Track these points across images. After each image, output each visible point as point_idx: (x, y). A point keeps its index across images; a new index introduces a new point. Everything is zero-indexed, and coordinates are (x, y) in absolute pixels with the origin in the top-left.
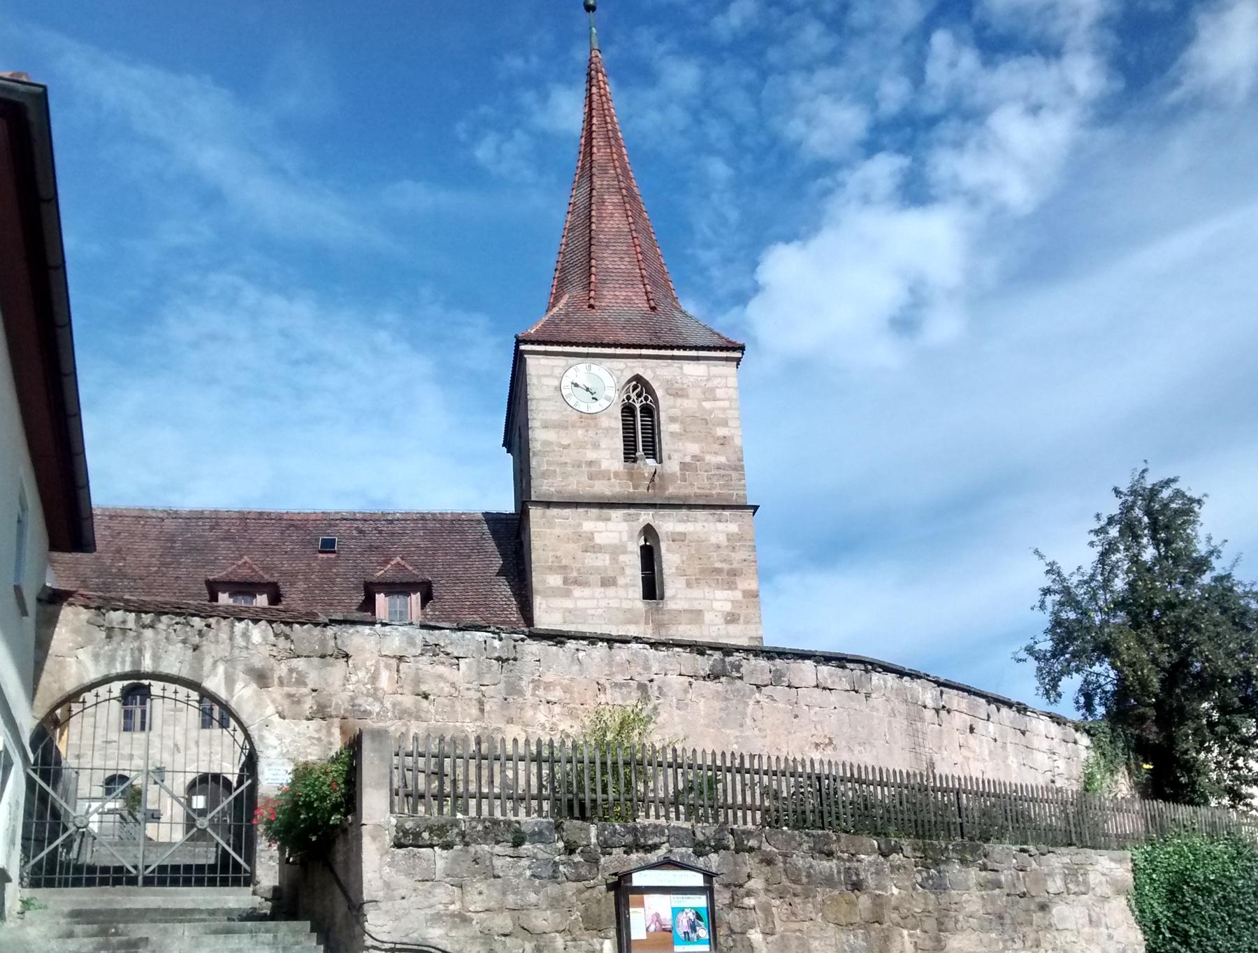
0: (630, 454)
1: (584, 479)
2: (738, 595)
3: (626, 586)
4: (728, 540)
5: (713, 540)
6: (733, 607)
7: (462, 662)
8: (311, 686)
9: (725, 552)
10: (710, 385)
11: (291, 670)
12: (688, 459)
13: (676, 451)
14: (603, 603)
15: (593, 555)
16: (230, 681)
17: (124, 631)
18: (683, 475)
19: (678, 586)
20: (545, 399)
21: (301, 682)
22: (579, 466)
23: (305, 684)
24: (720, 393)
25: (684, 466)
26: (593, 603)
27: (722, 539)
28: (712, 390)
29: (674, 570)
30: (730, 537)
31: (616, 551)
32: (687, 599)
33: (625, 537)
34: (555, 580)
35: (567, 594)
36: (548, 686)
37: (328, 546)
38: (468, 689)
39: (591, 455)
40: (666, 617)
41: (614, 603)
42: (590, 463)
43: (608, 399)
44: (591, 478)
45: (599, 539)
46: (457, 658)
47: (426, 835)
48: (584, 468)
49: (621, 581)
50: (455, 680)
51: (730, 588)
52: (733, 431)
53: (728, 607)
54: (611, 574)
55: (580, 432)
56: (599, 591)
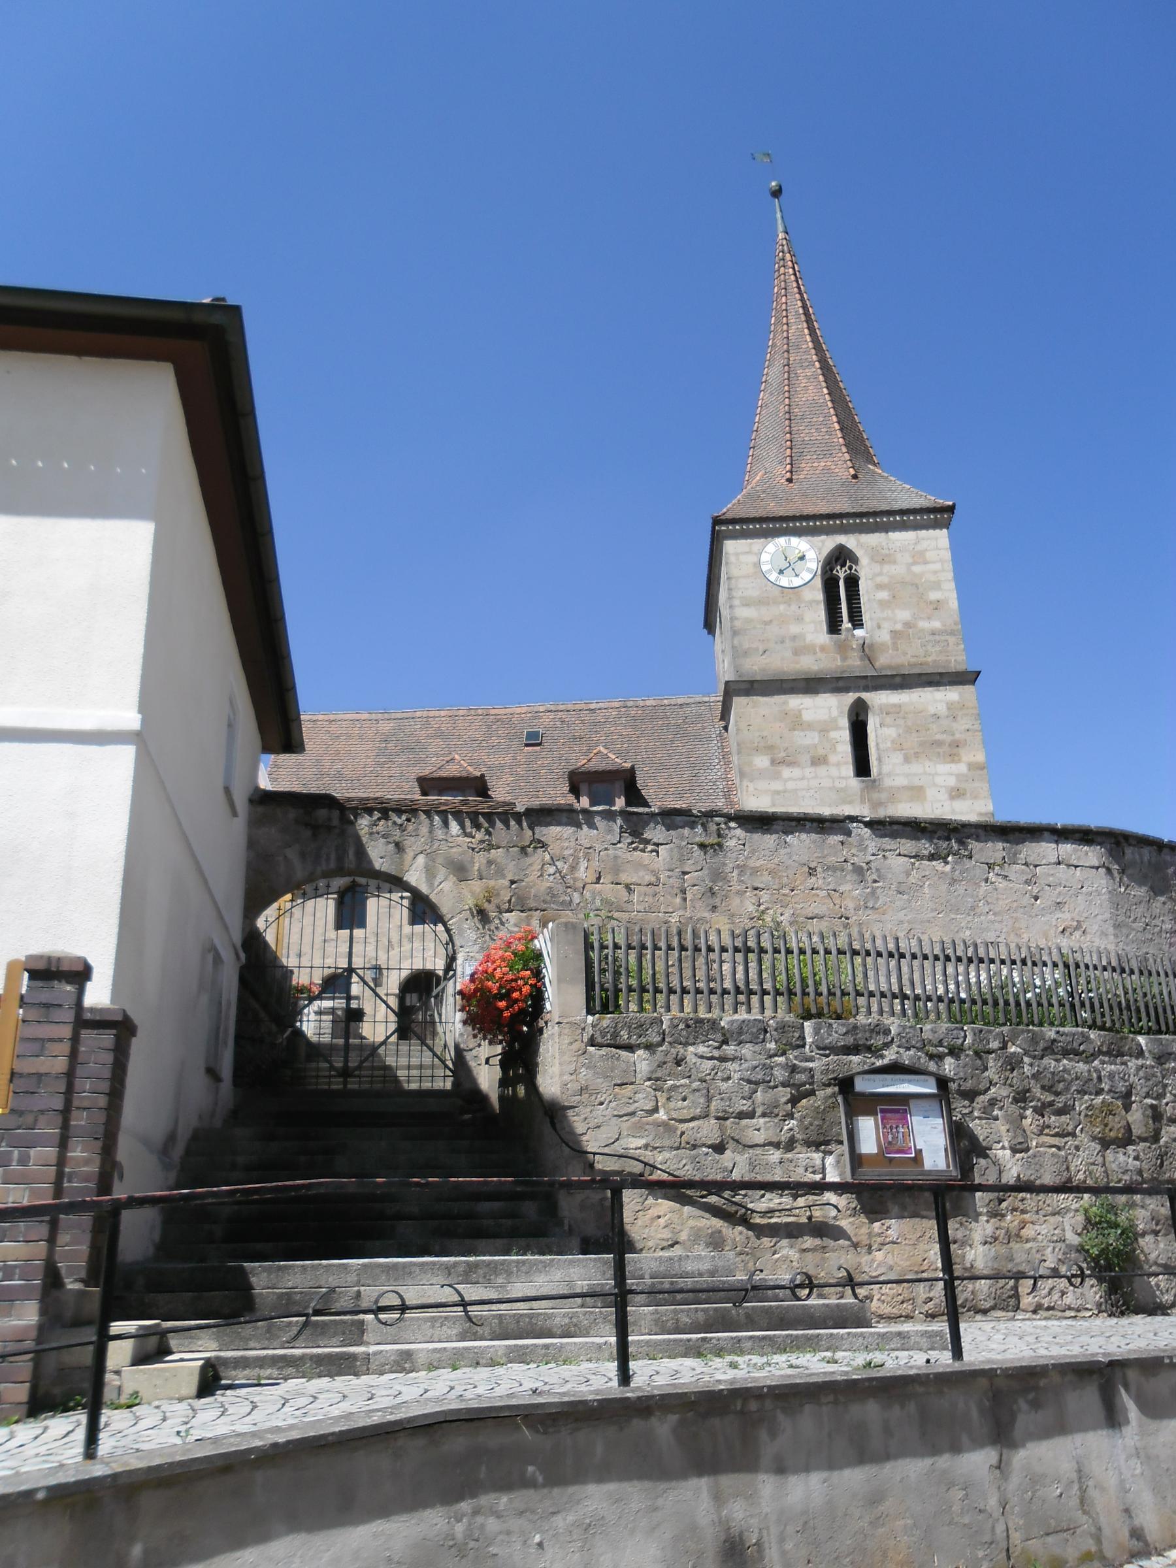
0: (834, 626)
1: (788, 654)
2: (962, 768)
3: (838, 765)
4: (949, 709)
5: (932, 710)
7: (661, 848)
8: (510, 877)
10: (919, 548)
11: (490, 863)
12: (899, 627)
13: (884, 619)
14: (814, 783)
15: (802, 734)
16: (430, 873)
17: (329, 828)
18: (894, 644)
21: (500, 873)
22: (782, 642)
23: (503, 877)
24: (930, 555)
25: (895, 634)
26: (804, 784)
27: (942, 709)
28: (922, 553)
29: (889, 744)
30: (950, 706)
31: (824, 729)
32: (907, 775)
33: (835, 713)
34: (762, 762)
35: (777, 776)
36: (755, 871)
37: (534, 740)
38: (669, 877)
39: (794, 629)
41: (827, 783)
42: (794, 638)
43: (809, 570)
44: (796, 652)
46: (658, 845)
47: (624, 1034)
49: (833, 759)
50: (655, 866)
51: (953, 761)
53: (952, 782)
54: (821, 752)
55: (782, 607)
56: (809, 771)
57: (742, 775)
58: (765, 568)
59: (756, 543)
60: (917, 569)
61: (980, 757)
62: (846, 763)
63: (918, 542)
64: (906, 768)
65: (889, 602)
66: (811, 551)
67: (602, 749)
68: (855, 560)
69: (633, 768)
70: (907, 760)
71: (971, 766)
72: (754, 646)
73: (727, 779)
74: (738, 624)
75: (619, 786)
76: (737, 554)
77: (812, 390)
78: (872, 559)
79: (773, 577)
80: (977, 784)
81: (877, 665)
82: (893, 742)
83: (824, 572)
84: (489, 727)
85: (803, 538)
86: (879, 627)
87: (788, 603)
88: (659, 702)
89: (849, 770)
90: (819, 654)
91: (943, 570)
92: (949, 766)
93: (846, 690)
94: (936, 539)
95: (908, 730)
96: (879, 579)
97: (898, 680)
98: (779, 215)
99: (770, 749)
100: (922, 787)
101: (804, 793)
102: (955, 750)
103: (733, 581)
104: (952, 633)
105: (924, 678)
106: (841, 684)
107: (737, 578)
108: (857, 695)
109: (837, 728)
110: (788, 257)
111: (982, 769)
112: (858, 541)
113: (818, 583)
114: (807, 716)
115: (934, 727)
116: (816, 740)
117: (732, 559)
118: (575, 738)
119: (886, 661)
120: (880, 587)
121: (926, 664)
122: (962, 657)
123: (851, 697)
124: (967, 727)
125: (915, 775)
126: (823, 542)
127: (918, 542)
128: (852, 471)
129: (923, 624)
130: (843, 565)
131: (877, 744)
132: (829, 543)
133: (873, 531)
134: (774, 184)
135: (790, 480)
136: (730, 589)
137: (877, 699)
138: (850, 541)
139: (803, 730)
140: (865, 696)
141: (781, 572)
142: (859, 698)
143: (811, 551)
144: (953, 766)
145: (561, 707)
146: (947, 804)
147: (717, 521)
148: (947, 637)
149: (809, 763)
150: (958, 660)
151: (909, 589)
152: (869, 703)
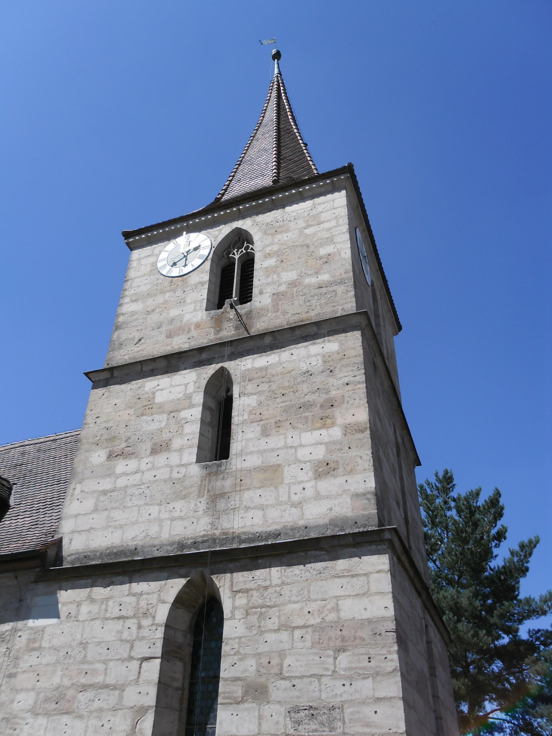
2: (336, 433)
3: (180, 450)
4: (325, 362)
5: (304, 367)
6: (330, 451)
9: (318, 379)
12: (283, 288)
14: (149, 476)
15: (149, 418)
19: (251, 435)
25: (277, 296)
27: (316, 363)
30: (326, 359)
34: (98, 457)
35: (110, 474)
39: (174, 313)
40: (228, 483)
41: (163, 474)
42: (172, 321)
44: (169, 336)
45: (160, 398)
49: (177, 443)
51: (324, 426)
52: (338, 246)
53: (320, 453)
54: (166, 436)
58: (159, 265)
60: (308, 231)
63: (314, 206)
64: (263, 444)
65: (276, 267)
70: (265, 433)
71: (348, 429)
80: (354, 453)
82: (250, 413)
85: (203, 232)
92: (316, 433)
93: (209, 362)
94: (333, 200)
100: (279, 465)
102: (329, 412)
104: (342, 282)
105: (298, 332)
115: (305, 388)
120: (268, 256)
123: (211, 370)
124: (346, 380)
125: (273, 450)
126: (220, 231)
127: (314, 206)
133: (270, 210)
138: (245, 224)
142: (222, 368)
144: (324, 432)
149: (149, 452)
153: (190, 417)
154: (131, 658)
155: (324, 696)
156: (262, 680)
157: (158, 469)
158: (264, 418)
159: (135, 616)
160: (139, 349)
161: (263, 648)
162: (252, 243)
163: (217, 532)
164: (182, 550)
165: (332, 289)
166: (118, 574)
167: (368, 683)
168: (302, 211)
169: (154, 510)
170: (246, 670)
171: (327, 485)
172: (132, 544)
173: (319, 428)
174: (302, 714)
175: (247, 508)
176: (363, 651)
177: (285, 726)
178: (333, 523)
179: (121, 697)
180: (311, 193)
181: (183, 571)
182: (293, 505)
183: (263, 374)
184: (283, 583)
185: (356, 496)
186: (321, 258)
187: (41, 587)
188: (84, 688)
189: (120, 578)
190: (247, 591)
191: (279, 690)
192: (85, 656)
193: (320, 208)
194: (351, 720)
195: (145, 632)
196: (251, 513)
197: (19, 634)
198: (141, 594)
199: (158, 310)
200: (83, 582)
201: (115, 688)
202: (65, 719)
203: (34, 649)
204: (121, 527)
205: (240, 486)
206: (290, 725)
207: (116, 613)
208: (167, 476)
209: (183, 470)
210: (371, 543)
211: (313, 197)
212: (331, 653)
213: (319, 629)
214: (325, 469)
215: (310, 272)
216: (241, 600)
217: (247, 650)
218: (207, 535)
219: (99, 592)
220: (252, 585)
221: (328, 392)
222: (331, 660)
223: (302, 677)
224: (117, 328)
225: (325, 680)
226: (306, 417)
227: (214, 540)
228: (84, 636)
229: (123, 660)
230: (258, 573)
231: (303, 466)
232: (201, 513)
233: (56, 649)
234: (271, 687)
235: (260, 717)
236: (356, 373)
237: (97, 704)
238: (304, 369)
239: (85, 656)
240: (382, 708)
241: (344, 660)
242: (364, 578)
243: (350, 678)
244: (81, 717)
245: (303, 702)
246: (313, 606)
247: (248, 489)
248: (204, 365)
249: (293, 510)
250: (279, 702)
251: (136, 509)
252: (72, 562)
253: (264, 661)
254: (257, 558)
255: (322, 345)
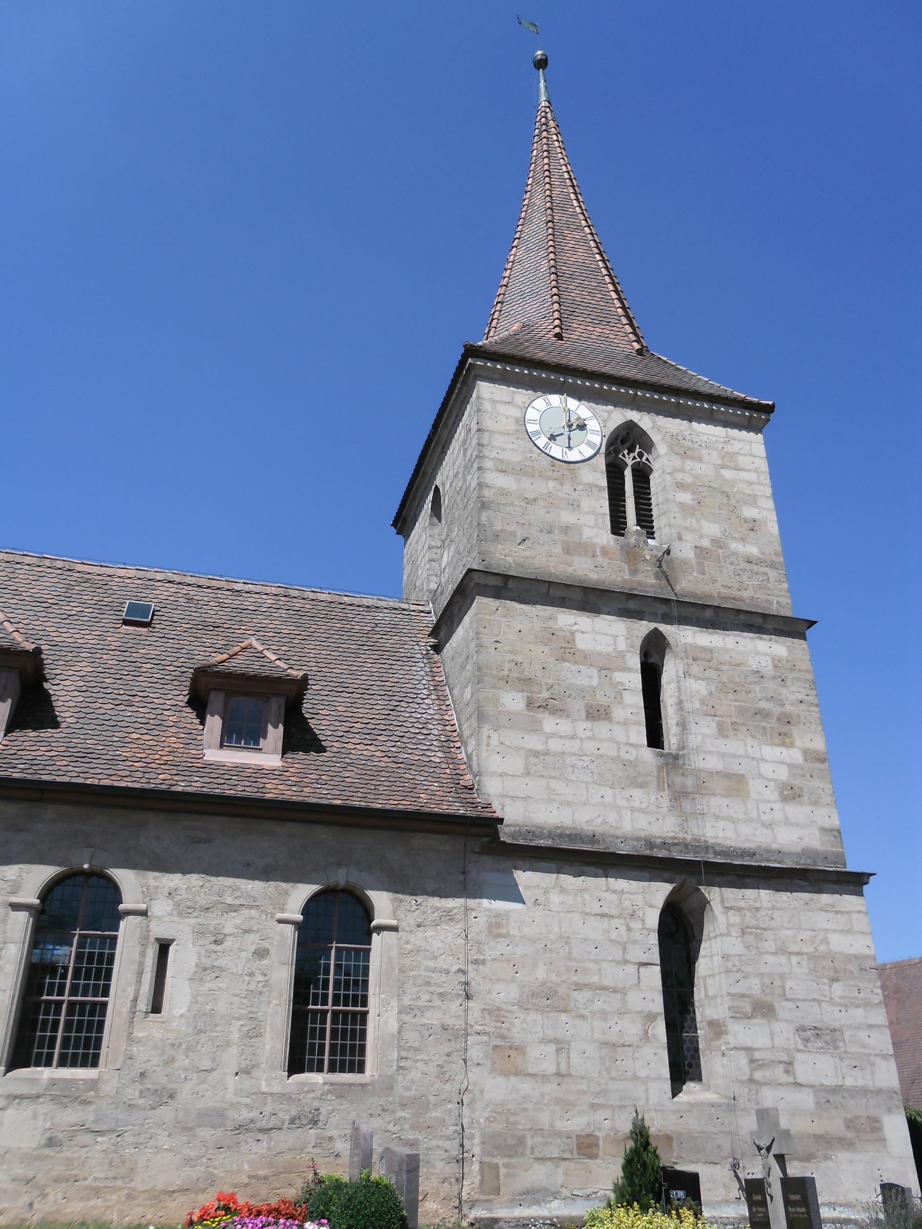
0: (618, 526)
1: (557, 549)
2: (796, 756)
3: (625, 723)
4: (775, 666)
5: (753, 664)
10: (728, 448)
12: (705, 543)
13: (686, 528)
18: (700, 564)
19: (707, 731)
20: (502, 433)
24: (742, 461)
26: (572, 746)
27: (766, 665)
29: (697, 705)
30: (777, 663)
31: (607, 666)
32: (723, 755)
33: (622, 645)
34: (513, 701)
35: (535, 728)
37: (139, 618)
39: (567, 517)
40: (689, 782)
41: (609, 750)
42: (566, 529)
43: (590, 444)
44: (568, 550)
48: (557, 536)
49: (618, 713)
51: (783, 744)
52: (764, 513)
53: (783, 774)
54: (601, 700)
55: (551, 484)
56: (583, 727)
57: (481, 717)
59: (522, 395)
60: (727, 474)
61: (819, 744)
62: (637, 723)
64: (721, 745)
66: (598, 421)
67: (255, 644)
68: (647, 445)
69: (305, 678)
70: (722, 731)
71: (808, 754)
72: (511, 528)
73: (444, 723)
74: (486, 492)
75: (276, 706)
76: (494, 402)
77: (581, 252)
78: (671, 448)
79: (542, 441)
80: (816, 783)
81: (678, 588)
82: (702, 702)
83: (607, 454)
84: (69, 587)
86: (680, 539)
87: (560, 481)
88: (336, 598)
89: (641, 736)
90: (600, 559)
91: (759, 483)
92: (778, 750)
94: (750, 443)
95: (723, 688)
96: (680, 476)
97: (709, 614)
98: (542, 85)
99: (526, 682)
100: (743, 776)
101: (574, 760)
102: (786, 729)
103: (486, 435)
104: (772, 565)
105: (742, 617)
106: (632, 605)
107: (492, 432)
108: (653, 625)
109: (625, 669)
110: (552, 124)
111: (823, 761)
112: (654, 422)
113: (601, 462)
114: (583, 643)
116: (595, 682)
117: (487, 406)
118: (205, 626)
119: (689, 584)
120: (681, 486)
121: (741, 599)
122: (786, 600)
123: (644, 627)
124: (800, 696)
125: (734, 756)
126: (609, 412)
128: (636, 346)
129: (734, 546)
130: (631, 450)
131: (680, 702)
132: (618, 416)
133: (674, 416)
134: (539, 52)
135: (559, 336)
136: (480, 445)
137: (682, 636)
138: (645, 421)
139: (576, 663)
140: (663, 628)
141: (552, 438)
143: (598, 421)
144: (783, 750)
145: (189, 580)
146: (778, 806)
147: (471, 351)
148: (767, 570)
149: (583, 714)
150: (779, 599)
151: (715, 496)
152: (671, 640)
153: (628, 684)
154: (626, 962)
155: (825, 1019)
156: (768, 999)
157: (601, 741)
158: (718, 713)
159: (620, 916)
160: (527, 553)
161: (764, 969)
162: (649, 452)
163: (689, 837)
164: (651, 849)
165: (762, 569)
166: (589, 864)
167: (860, 1012)
168: (714, 439)
169: (608, 793)
170: (750, 988)
171: (796, 811)
172: (588, 828)
173: (779, 745)
174: (809, 1033)
175: (717, 817)
176: (852, 982)
177: (796, 1043)
178: (806, 852)
179: (624, 1002)
180: (722, 417)
181: (666, 875)
182: (764, 825)
183: (709, 656)
184: (773, 908)
185: (823, 830)
186: (745, 521)
187: (487, 860)
188: (579, 987)
189: (592, 869)
190: (739, 909)
191: (784, 1009)
192: (570, 953)
193: (735, 447)
194: (850, 1041)
195: (637, 936)
196: (721, 824)
197: (474, 914)
198: (622, 892)
199: (541, 503)
200: (544, 865)
201: (615, 991)
202: (564, 1017)
203: (500, 935)
204: (569, 804)
205: (701, 789)
206: (800, 1042)
207: (596, 909)
208: (615, 754)
209: (633, 752)
210: (849, 883)
211: (726, 424)
212: (826, 981)
213: (813, 957)
214: (790, 793)
215: (735, 535)
216: (735, 918)
217: (749, 969)
218: (678, 838)
219: (567, 880)
220: (742, 904)
221: (783, 705)
222: (827, 988)
223: (804, 1000)
224: (484, 506)
225: (825, 1005)
226: (764, 728)
227: (686, 845)
228: (564, 930)
229: (618, 963)
230: (749, 893)
231: (767, 783)
232: (665, 810)
233: (532, 941)
234: (777, 1007)
235: (772, 1033)
236: (809, 692)
237: (597, 1005)
238: (754, 667)
239: (570, 953)
240: (874, 1034)
241: (838, 989)
242: (846, 916)
243: (845, 1005)
244: (583, 1017)
245: (809, 1023)
246: (806, 935)
247: (714, 795)
248: (632, 617)
249: (765, 831)
250: (786, 1021)
251: (584, 785)
252: (512, 835)
253: (767, 981)
254: (744, 876)
255: (769, 644)
